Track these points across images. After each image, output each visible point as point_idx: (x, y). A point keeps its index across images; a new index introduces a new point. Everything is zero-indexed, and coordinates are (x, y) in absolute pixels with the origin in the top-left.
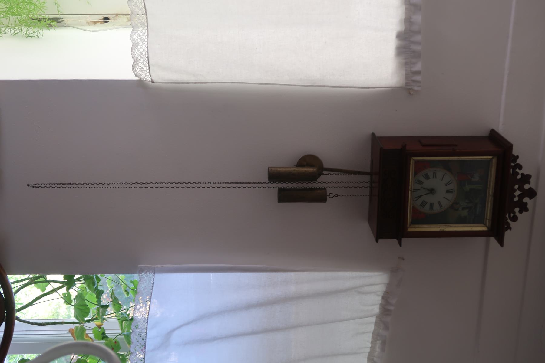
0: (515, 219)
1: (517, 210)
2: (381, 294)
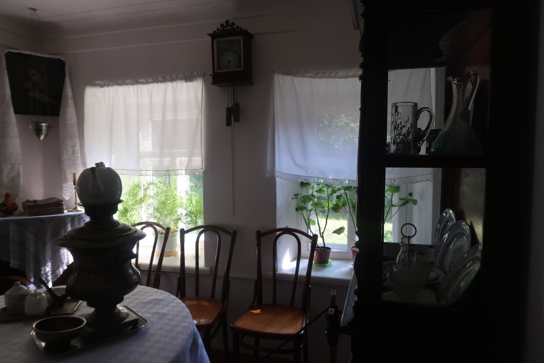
0: (238, 26)
1: (234, 26)
2: (283, 76)
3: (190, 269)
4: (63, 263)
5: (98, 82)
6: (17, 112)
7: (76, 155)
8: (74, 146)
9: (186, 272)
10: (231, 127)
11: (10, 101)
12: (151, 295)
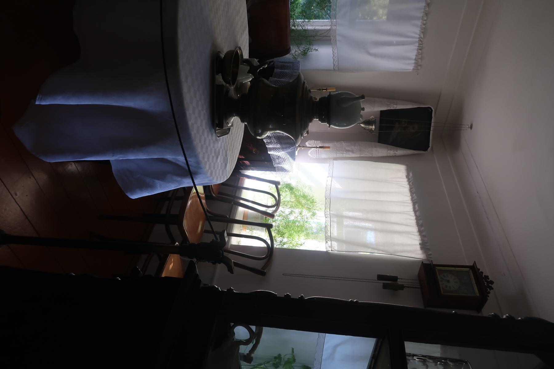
0: (489, 293)
3: (232, 228)
5: (411, 174)
6: (383, 113)
7: (345, 152)
8: (352, 152)
9: (229, 224)
10: (377, 279)
11: (392, 108)
12: (230, 163)
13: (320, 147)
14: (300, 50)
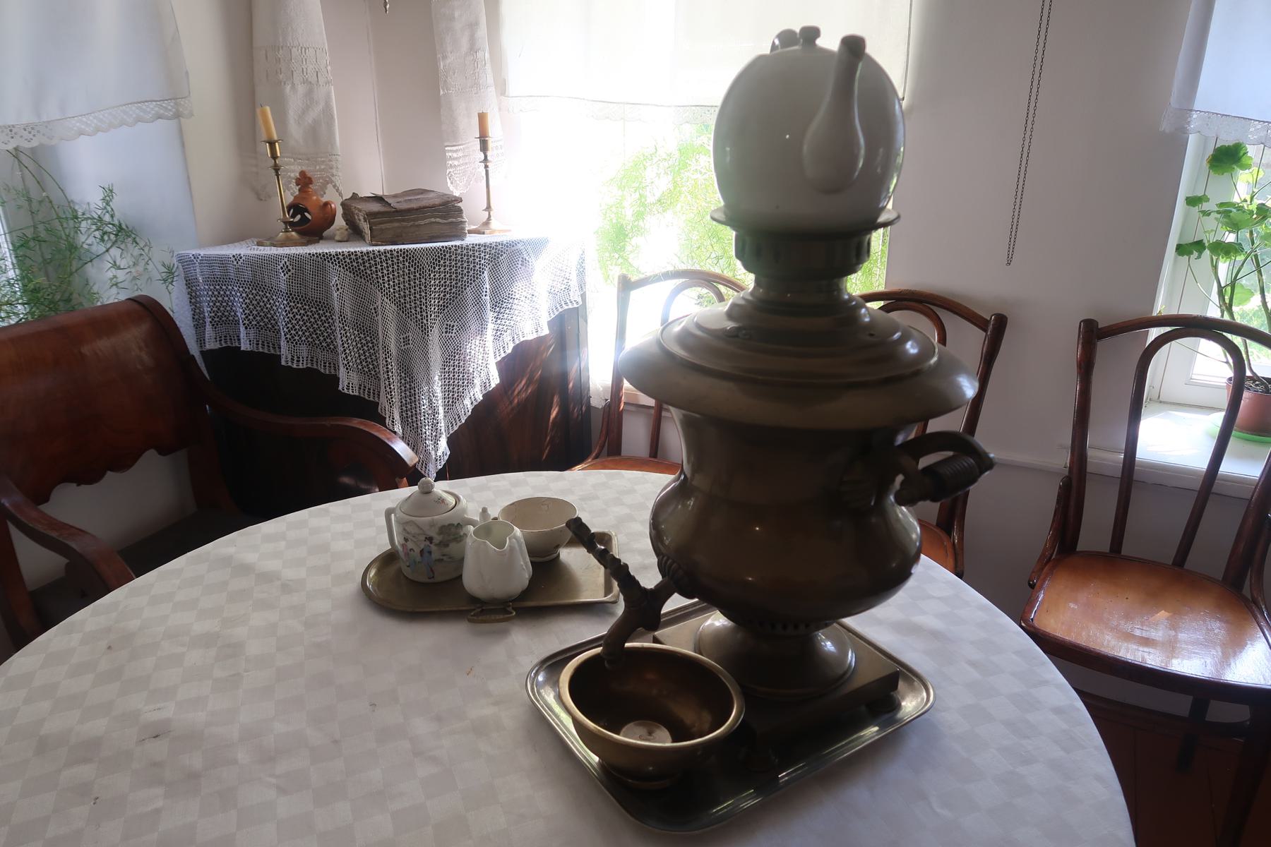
4: (471, 383)
7: (480, 54)
8: (473, 26)
13: (484, 147)
14: (107, 251)
